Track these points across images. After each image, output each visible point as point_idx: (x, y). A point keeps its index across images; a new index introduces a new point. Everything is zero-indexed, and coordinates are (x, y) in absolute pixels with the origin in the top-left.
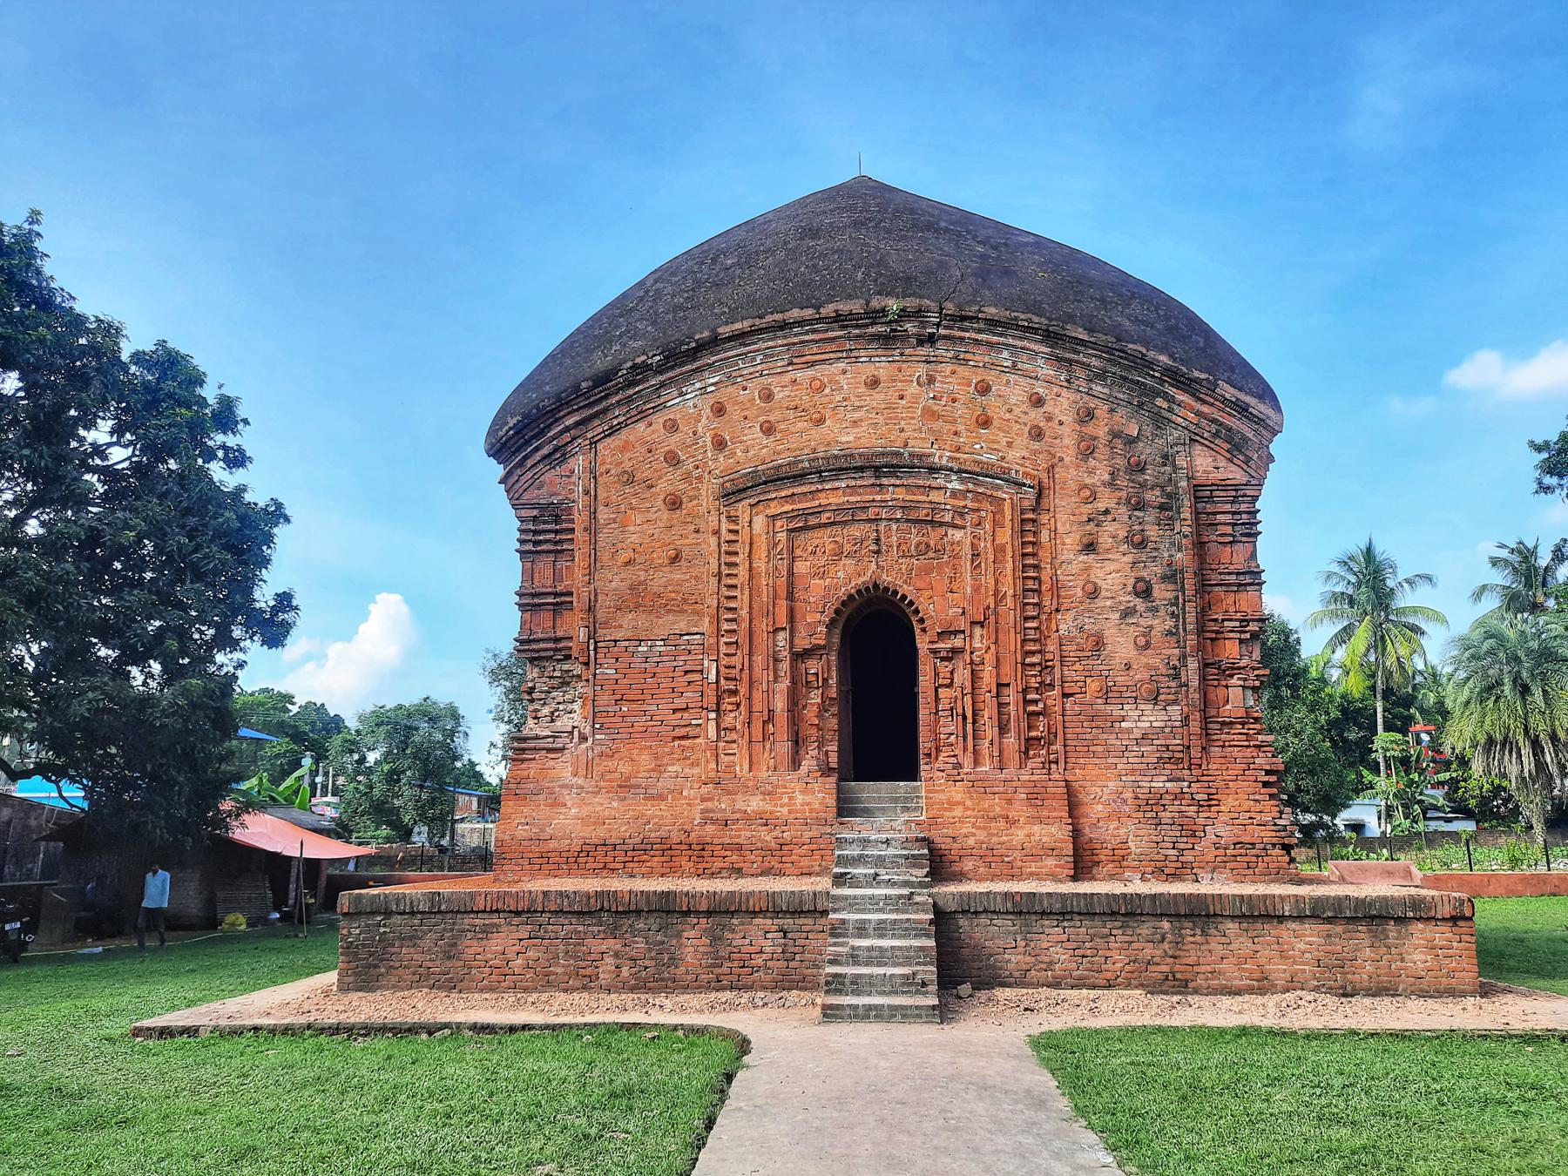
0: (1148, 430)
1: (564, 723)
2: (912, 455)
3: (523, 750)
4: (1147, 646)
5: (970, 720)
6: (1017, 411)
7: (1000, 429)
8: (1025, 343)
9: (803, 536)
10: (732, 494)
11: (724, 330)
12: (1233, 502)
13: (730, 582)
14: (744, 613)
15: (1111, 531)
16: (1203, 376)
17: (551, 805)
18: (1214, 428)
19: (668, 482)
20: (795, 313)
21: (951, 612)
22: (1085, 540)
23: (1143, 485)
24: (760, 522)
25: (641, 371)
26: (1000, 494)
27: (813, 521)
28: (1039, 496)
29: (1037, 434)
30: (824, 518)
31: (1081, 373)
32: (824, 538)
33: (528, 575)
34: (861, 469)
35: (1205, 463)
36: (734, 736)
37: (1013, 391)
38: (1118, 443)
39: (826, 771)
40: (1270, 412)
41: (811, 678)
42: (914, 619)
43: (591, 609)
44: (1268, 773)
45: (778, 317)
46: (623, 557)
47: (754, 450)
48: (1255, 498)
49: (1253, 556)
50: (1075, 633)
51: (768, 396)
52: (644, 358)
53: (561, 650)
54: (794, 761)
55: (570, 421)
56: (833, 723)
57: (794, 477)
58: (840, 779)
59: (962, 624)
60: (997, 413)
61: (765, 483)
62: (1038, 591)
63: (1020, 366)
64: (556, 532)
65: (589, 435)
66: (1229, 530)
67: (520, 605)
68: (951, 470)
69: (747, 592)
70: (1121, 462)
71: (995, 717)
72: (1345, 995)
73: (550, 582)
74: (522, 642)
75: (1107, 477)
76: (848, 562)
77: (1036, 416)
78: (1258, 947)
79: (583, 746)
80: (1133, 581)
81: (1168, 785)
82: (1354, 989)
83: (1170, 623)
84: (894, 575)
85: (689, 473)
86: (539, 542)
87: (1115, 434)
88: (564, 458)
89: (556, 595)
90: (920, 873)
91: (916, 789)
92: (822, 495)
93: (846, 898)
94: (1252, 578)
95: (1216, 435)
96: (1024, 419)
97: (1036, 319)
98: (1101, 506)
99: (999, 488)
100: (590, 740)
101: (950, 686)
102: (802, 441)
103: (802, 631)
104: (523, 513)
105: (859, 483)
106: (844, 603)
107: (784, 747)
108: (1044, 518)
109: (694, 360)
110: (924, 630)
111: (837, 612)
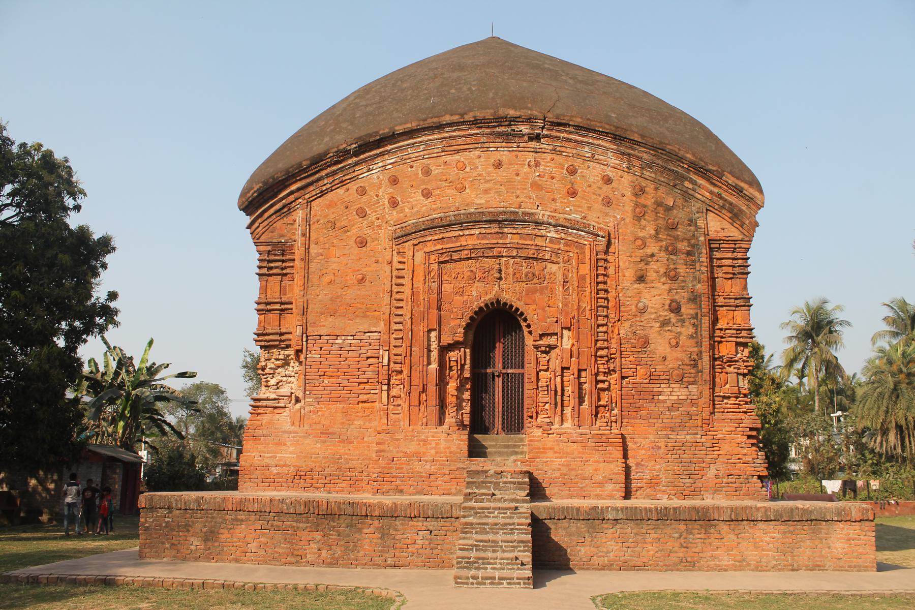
0: (680, 202)
1: (285, 390)
2: (524, 214)
3: (258, 407)
4: (677, 345)
5: (559, 393)
6: (594, 186)
7: (583, 198)
8: (600, 142)
9: (448, 266)
10: (401, 238)
11: (399, 129)
12: (733, 252)
13: (399, 296)
14: (407, 318)
15: (655, 269)
16: (714, 168)
17: (277, 444)
18: (721, 202)
19: (359, 228)
20: (447, 119)
21: (548, 320)
22: (638, 274)
23: (676, 238)
24: (419, 256)
25: (344, 154)
26: (582, 241)
27: (456, 256)
28: (609, 244)
29: (608, 202)
30: (464, 254)
31: (636, 163)
33: (264, 289)
34: (490, 222)
35: (716, 225)
36: (399, 402)
37: (591, 174)
38: (661, 209)
39: (461, 425)
40: (757, 194)
41: (452, 364)
42: (523, 324)
43: (304, 312)
44: (751, 429)
45: (435, 120)
46: (326, 279)
47: (417, 207)
48: (747, 249)
49: (745, 287)
50: (630, 336)
51: (427, 172)
52: (344, 146)
53: (284, 341)
54: (440, 419)
55: (294, 187)
56: (467, 395)
57: (444, 226)
58: (471, 434)
59: (556, 329)
60: (581, 187)
61: (424, 230)
62: (607, 307)
63: (596, 156)
64: (283, 261)
65: (307, 196)
66: (730, 270)
67: (258, 310)
68: (550, 224)
69: (410, 304)
70: (661, 222)
71: (576, 391)
72: (793, 570)
73: (277, 295)
74: (258, 335)
75: (653, 232)
77: (606, 189)
78: (740, 540)
79: (298, 406)
80: (668, 302)
81: (688, 437)
82: (798, 565)
83: (691, 330)
84: (510, 293)
85: (373, 223)
86: (271, 268)
87: (659, 204)
88: (289, 212)
89: (282, 303)
90: (523, 494)
91: (522, 440)
92: (462, 239)
93: (474, 508)
94: (745, 302)
95: (723, 207)
96: (599, 192)
97: (607, 127)
98: (649, 251)
99: (583, 237)
100: (303, 401)
101: (546, 370)
102: (449, 202)
103: (446, 329)
104: (262, 248)
105: (488, 231)
106: (476, 313)
107: (433, 410)
108: (610, 258)
109: (379, 148)
110: (530, 332)
111: (471, 318)
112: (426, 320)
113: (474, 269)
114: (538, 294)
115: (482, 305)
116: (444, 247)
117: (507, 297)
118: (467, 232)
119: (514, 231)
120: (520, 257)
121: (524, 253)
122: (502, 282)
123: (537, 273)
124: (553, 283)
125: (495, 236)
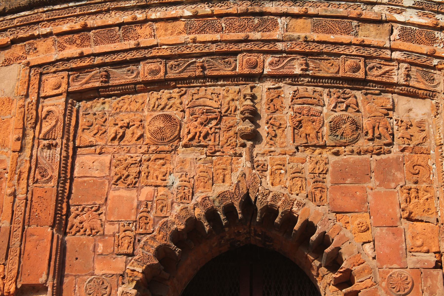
9: (98, 106)
21: (411, 261)
27: (120, 77)
30: (144, 71)
32: (144, 109)
76: (191, 155)
84: (284, 177)
92: (145, 30)
106: (176, 236)
111: (162, 253)
112: (14, 258)
113: (178, 116)
114: (373, 183)
115: (199, 212)
116: (87, 50)
117: (277, 189)
118: (154, 14)
119: (296, 10)
120: (316, 80)
121: (326, 68)
122: (258, 149)
123: (366, 123)
124: (419, 149)
125: (237, 22)
